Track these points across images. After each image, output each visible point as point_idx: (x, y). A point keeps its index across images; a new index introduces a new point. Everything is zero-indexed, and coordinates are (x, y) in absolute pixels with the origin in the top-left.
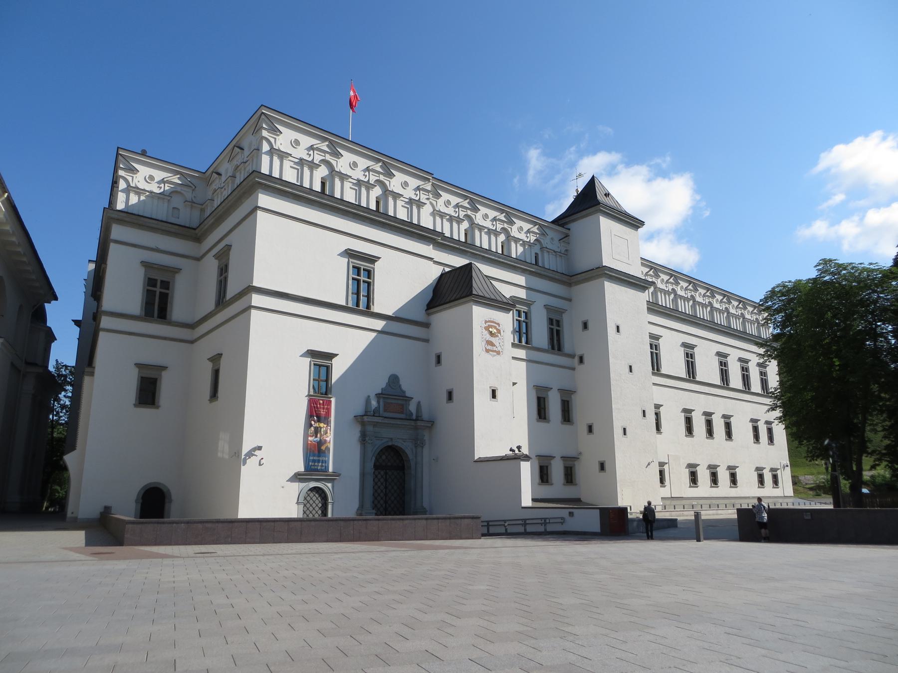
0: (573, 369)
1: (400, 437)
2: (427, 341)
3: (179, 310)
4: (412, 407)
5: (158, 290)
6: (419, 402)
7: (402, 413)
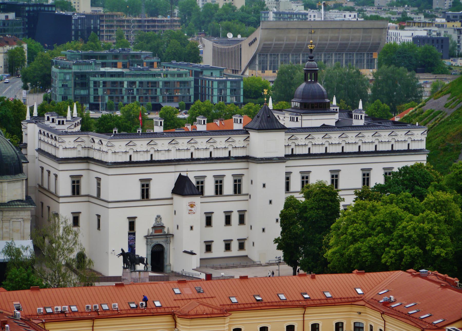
0: (247, 200)
1: (161, 241)
2: (172, 204)
3: (83, 191)
4: (166, 230)
5: (76, 184)
6: (168, 228)
7: (161, 232)
